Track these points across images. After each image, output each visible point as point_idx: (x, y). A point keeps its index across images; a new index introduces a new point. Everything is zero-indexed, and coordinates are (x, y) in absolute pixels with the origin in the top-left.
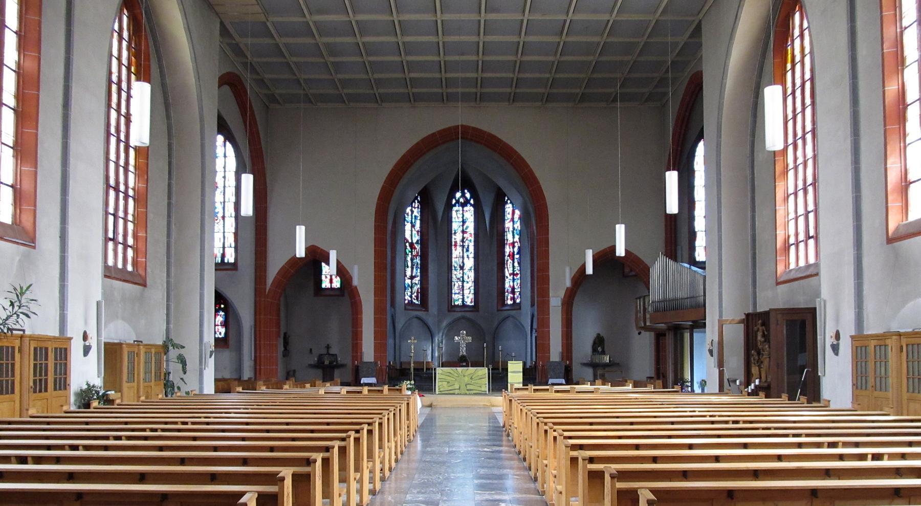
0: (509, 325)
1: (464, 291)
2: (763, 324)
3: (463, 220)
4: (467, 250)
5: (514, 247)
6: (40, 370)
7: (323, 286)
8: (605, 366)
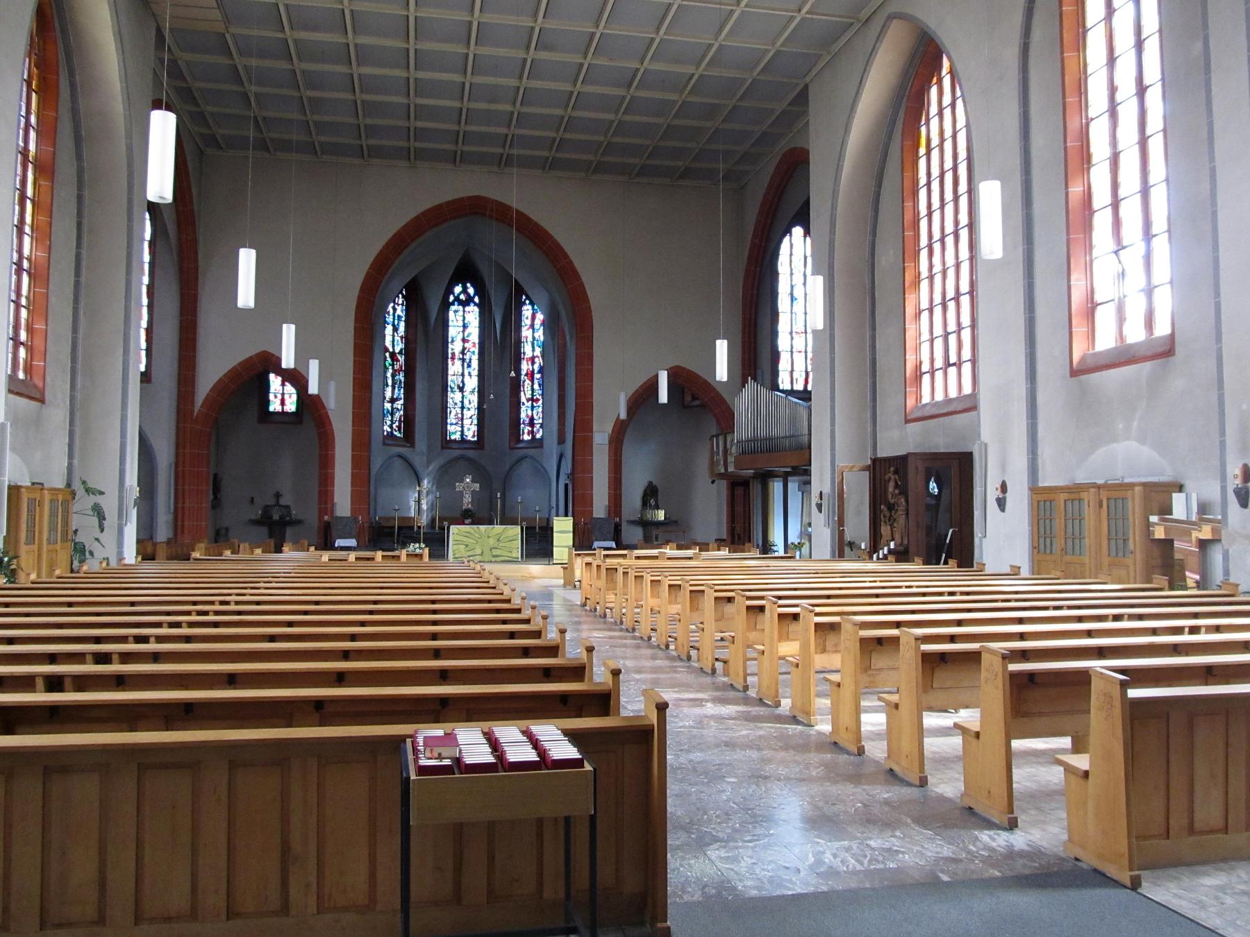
0: (525, 467)
1: (463, 420)
2: (896, 472)
3: (464, 324)
4: (469, 366)
5: (533, 363)
7: (271, 409)
8: (659, 524)
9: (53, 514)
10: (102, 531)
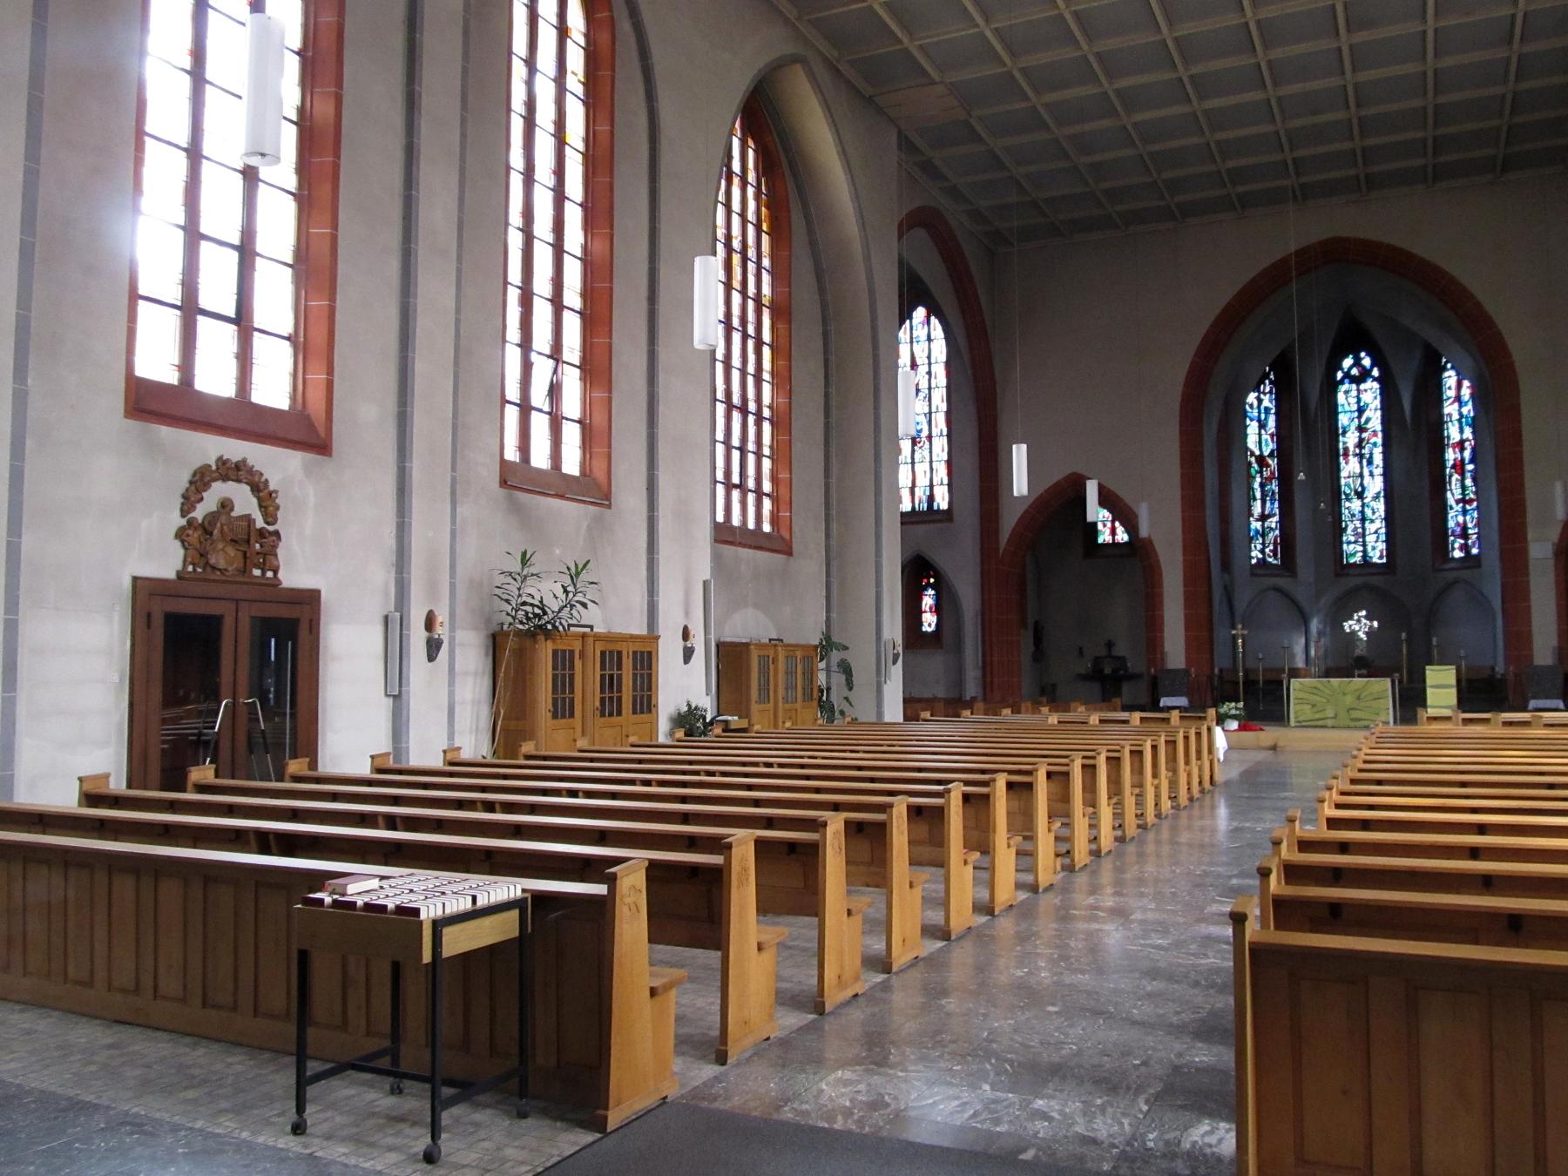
1: (1367, 536)
3: (1360, 405)
4: (1370, 462)
5: (1462, 449)
6: (610, 684)
7: (1100, 541)
9: (790, 673)
10: (851, 689)
